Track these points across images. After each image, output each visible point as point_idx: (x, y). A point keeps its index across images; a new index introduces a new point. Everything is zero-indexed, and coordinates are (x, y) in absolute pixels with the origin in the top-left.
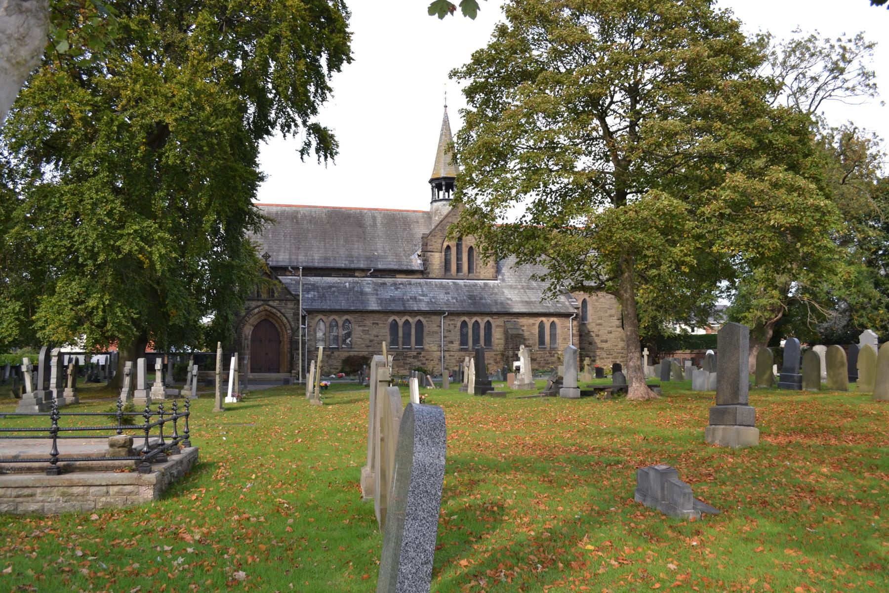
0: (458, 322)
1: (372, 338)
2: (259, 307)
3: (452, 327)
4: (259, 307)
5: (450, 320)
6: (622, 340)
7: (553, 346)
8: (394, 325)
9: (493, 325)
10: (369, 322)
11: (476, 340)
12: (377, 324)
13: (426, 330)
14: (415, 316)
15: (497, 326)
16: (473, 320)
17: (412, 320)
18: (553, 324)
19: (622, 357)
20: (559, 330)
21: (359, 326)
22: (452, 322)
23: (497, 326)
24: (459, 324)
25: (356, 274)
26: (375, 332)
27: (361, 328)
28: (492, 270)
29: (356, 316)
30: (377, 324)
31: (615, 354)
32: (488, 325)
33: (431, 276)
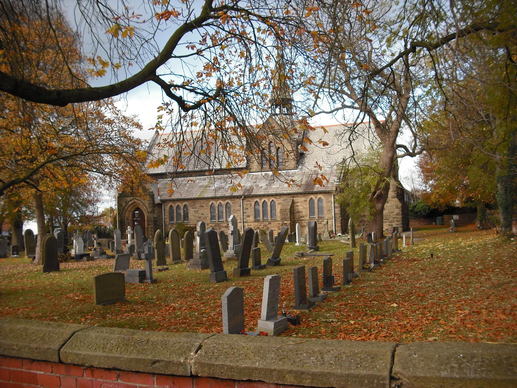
0: (253, 201)
1: (200, 216)
2: (131, 200)
3: (249, 206)
4: (131, 200)
5: (248, 201)
6: (397, 207)
7: (320, 216)
8: (212, 206)
9: (277, 203)
10: (197, 205)
11: (265, 214)
12: (203, 206)
13: (232, 208)
14: (225, 200)
15: (279, 204)
16: (177, 205)
17: (224, 203)
18: (320, 200)
19: (397, 221)
20: (325, 204)
21: (193, 208)
22: (249, 203)
23: (279, 204)
24: (253, 204)
25: (206, 174)
26: (202, 211)
27: (193, 210)
28: (294, 162)
29: (190, 202)
30: (203, 206)
31: (391, 219)
32: (273, 203)
33: (252, 171)
